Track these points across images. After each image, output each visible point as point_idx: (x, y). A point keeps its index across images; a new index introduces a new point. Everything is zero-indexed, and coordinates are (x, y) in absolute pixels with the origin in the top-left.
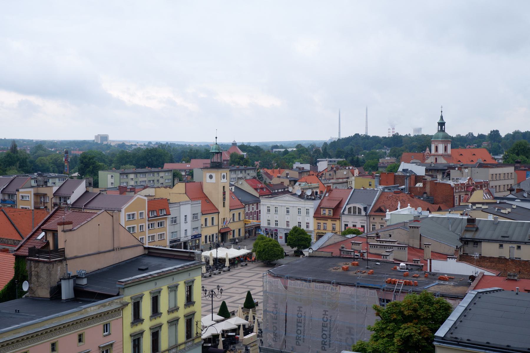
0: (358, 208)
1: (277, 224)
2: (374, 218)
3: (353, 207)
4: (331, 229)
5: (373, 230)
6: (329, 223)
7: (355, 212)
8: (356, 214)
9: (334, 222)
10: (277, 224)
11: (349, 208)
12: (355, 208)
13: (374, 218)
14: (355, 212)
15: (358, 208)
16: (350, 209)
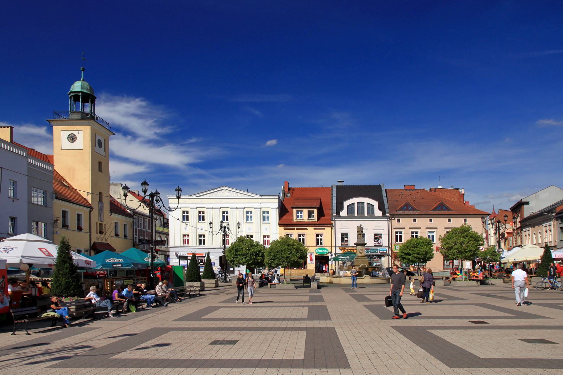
0: (367, 203)
1: (202, 242)
2: (399, 221)
3: (358, 203)
4: (315, 244)
5: (397, 241)
6: (310, 235)
7: (361, 211)
8: (363, 214)
9: (319, 232)
10: (202, 242)
11: (348, 206)
12: (360, 204)
13: (399, 221)
14: (361, 211)
15: (367, 203)
16: (351, 207)
